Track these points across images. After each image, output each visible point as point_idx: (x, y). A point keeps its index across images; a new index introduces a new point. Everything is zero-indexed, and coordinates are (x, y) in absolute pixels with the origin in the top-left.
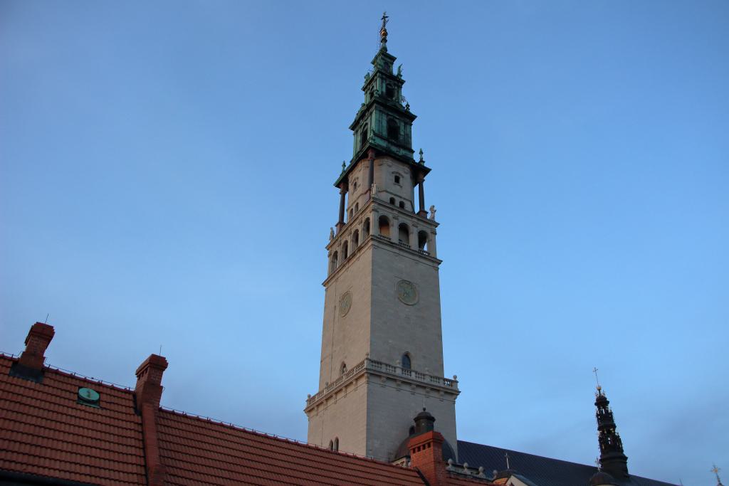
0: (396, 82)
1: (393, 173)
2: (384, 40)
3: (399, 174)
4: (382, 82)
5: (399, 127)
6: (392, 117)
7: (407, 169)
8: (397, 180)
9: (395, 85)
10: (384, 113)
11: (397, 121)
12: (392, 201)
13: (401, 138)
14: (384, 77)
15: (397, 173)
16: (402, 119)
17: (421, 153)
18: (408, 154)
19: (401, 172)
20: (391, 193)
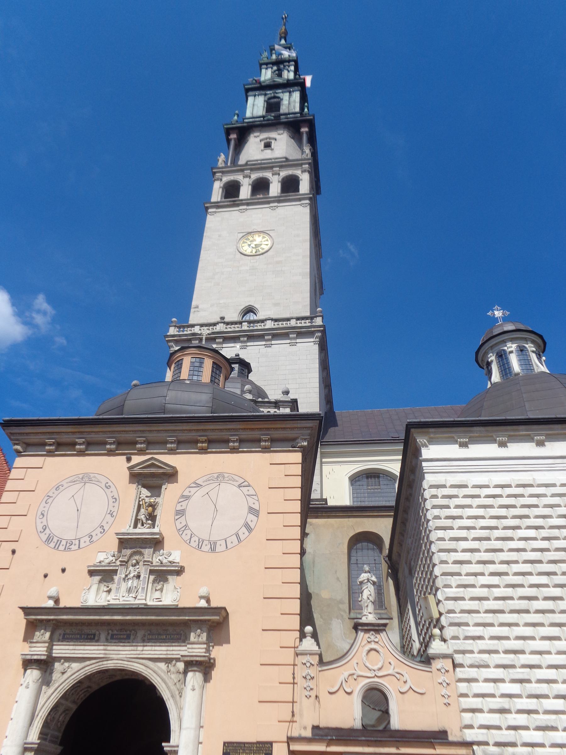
3: (270, 138)
6: (273, 95)
8: (268, 145)
14: (269, 66)
15: (266, 139)
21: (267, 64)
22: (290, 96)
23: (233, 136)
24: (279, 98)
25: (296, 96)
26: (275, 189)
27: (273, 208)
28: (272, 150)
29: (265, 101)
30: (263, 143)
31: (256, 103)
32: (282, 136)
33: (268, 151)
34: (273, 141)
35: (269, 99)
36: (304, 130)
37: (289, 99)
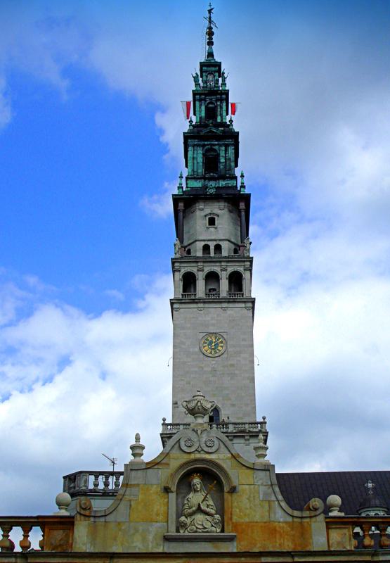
0: (219, 96)
1: (205, 216)
2: (210, 43)
4: (201, 106)
5: (218, 155)
6: (209, 147)
7: (222, 204)
8: (212, 222)
9: (217, 100)
10: (198, 146)
11: (216, 147)
12: (206, 248)
13: (221, 167)
14: (203, 97)
15: (210, 214)
16: (221, 143)
17: (242, 176)
18: (231, 183)
19: (216, 211)
20: (204, 240)
21: (200, 94)
22: (226, 150)
23: (181, 205)
24: (215, 150)
25: (231, 150)
26: (224, 285)
27: (224, 309)
28: (216, 228)
29: (203, 154)
30: (207, 218)
31: (195, 156)
32: (223, 211)
33: (212, 229)
34: (216, 218)
35: (207, 151)
36: (242, 206)
37: (226, 154)
